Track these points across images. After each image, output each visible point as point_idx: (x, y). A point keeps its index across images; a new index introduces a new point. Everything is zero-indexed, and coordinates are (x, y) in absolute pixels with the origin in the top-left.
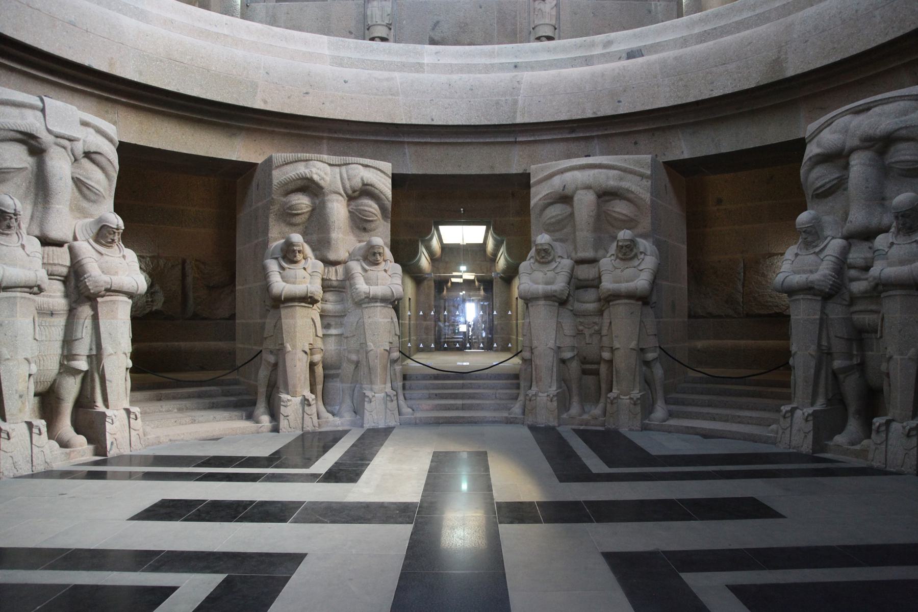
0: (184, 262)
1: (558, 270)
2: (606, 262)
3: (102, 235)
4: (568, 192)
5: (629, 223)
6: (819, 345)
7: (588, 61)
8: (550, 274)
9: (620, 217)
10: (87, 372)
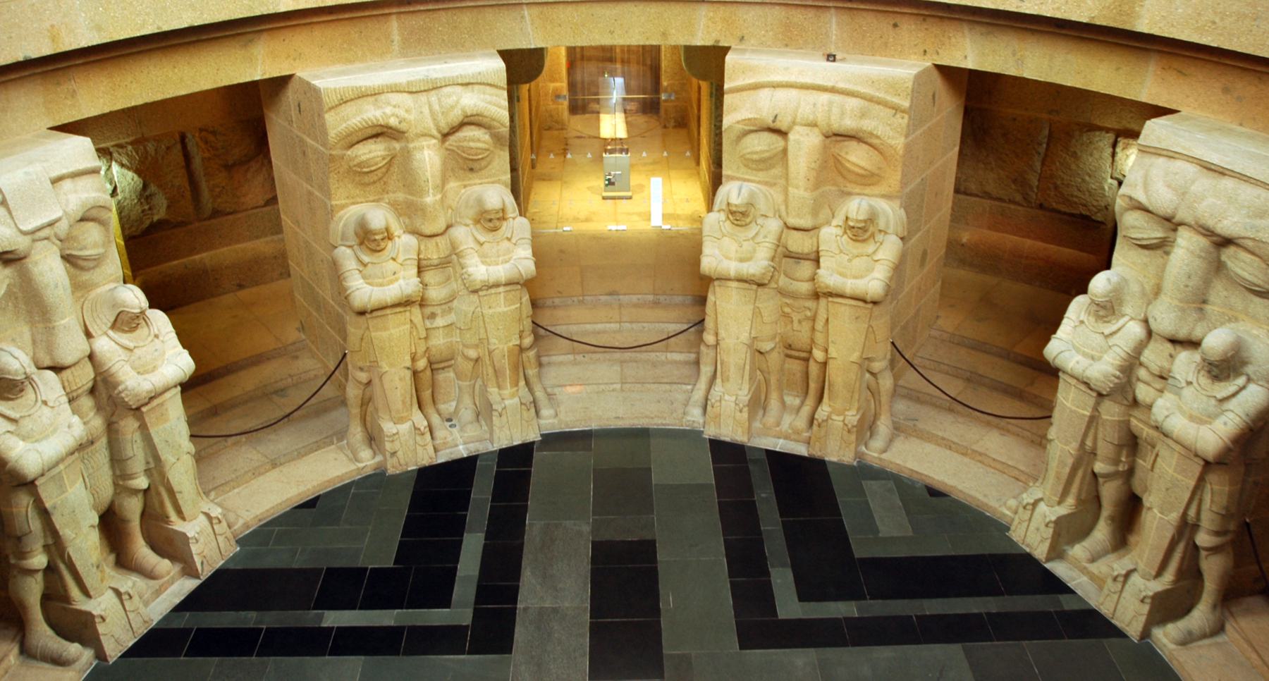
0: (183, 138)
1: (760, 239)
2: (830, 235)
3: (125, 322)
4: (782, 125)
5: (868, 179)
6: (1083, 443)
8: (747, 246)
9: (857, 170)
10: (146, 491)
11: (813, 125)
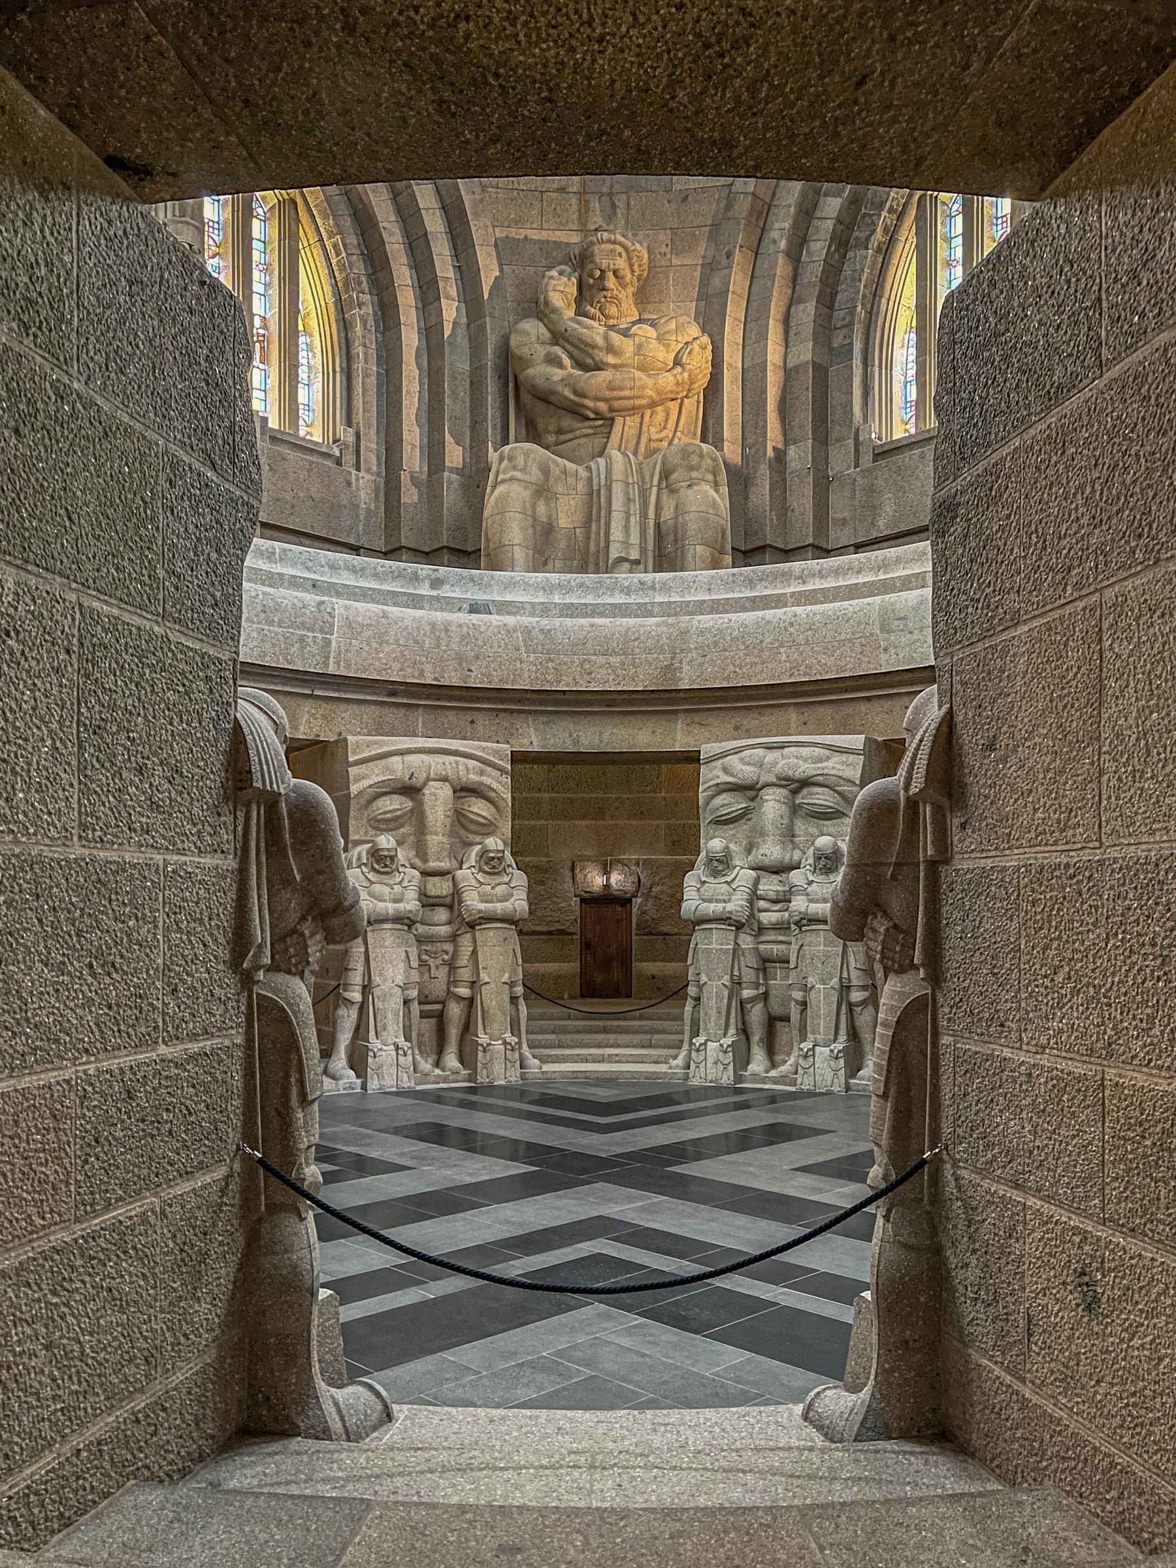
1: (405, 884)
5: (488, 828)
7: (416, 602)
11: (444, 779)
